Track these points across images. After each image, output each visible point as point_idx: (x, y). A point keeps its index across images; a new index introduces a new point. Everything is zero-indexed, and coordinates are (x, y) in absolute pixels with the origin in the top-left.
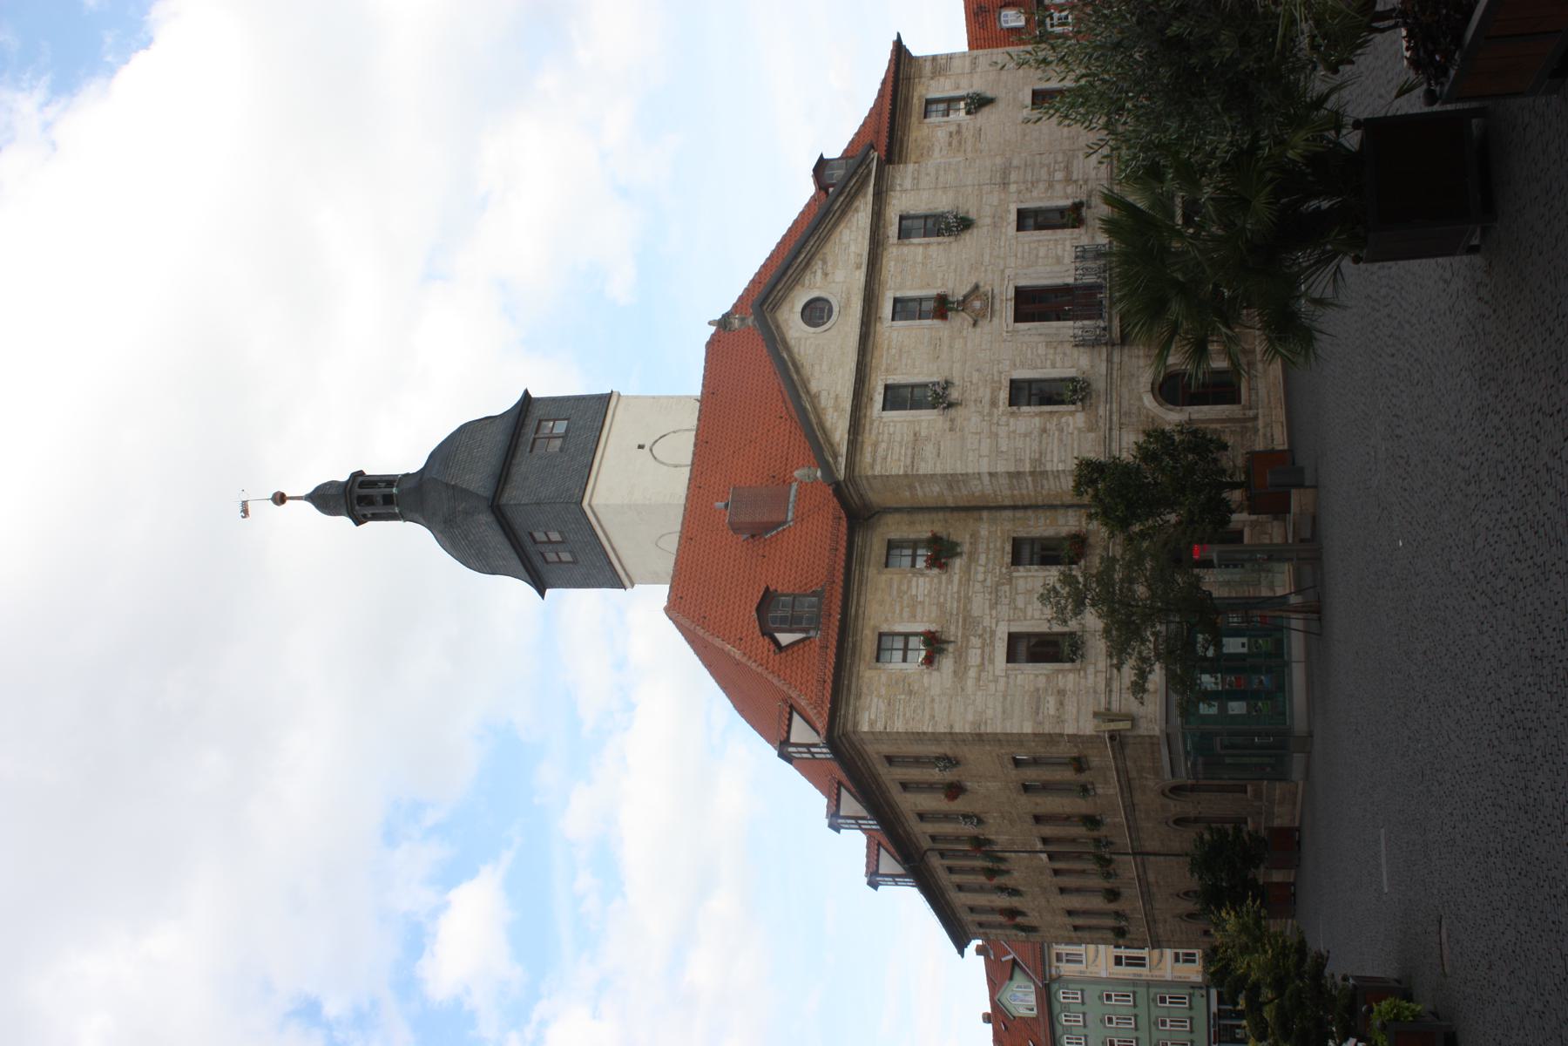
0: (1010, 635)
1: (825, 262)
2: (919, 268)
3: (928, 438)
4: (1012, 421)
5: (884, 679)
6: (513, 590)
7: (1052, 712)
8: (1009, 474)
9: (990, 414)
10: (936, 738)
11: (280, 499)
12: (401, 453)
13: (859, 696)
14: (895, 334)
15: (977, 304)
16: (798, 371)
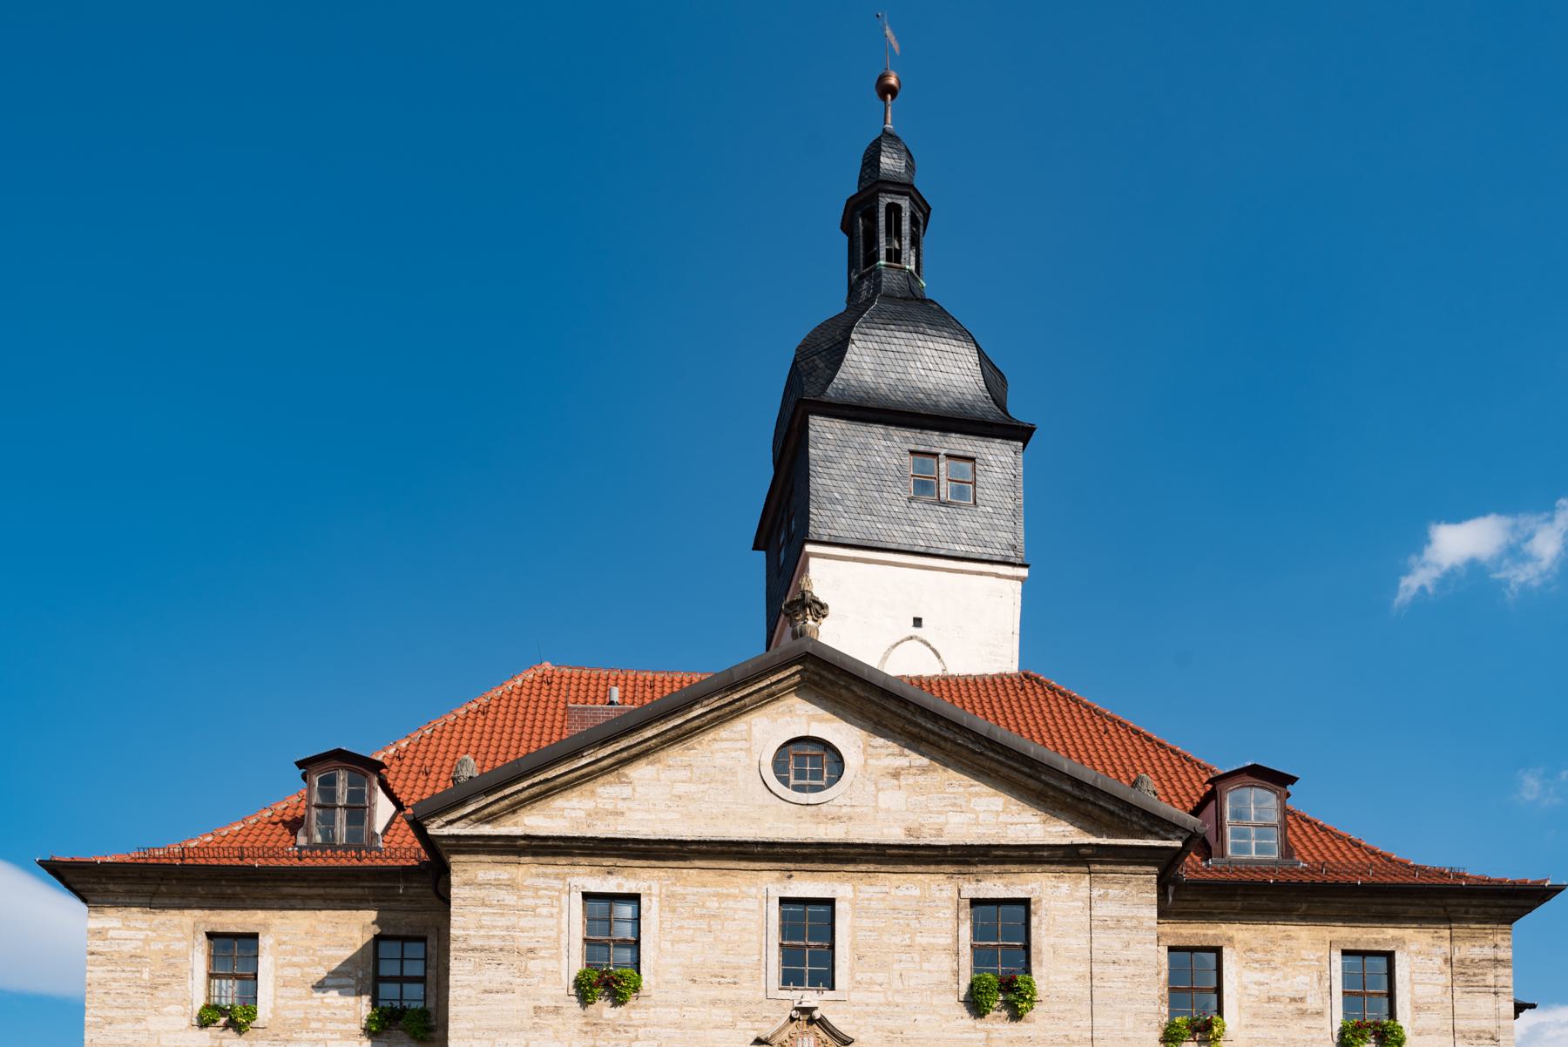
14: (752, 904)
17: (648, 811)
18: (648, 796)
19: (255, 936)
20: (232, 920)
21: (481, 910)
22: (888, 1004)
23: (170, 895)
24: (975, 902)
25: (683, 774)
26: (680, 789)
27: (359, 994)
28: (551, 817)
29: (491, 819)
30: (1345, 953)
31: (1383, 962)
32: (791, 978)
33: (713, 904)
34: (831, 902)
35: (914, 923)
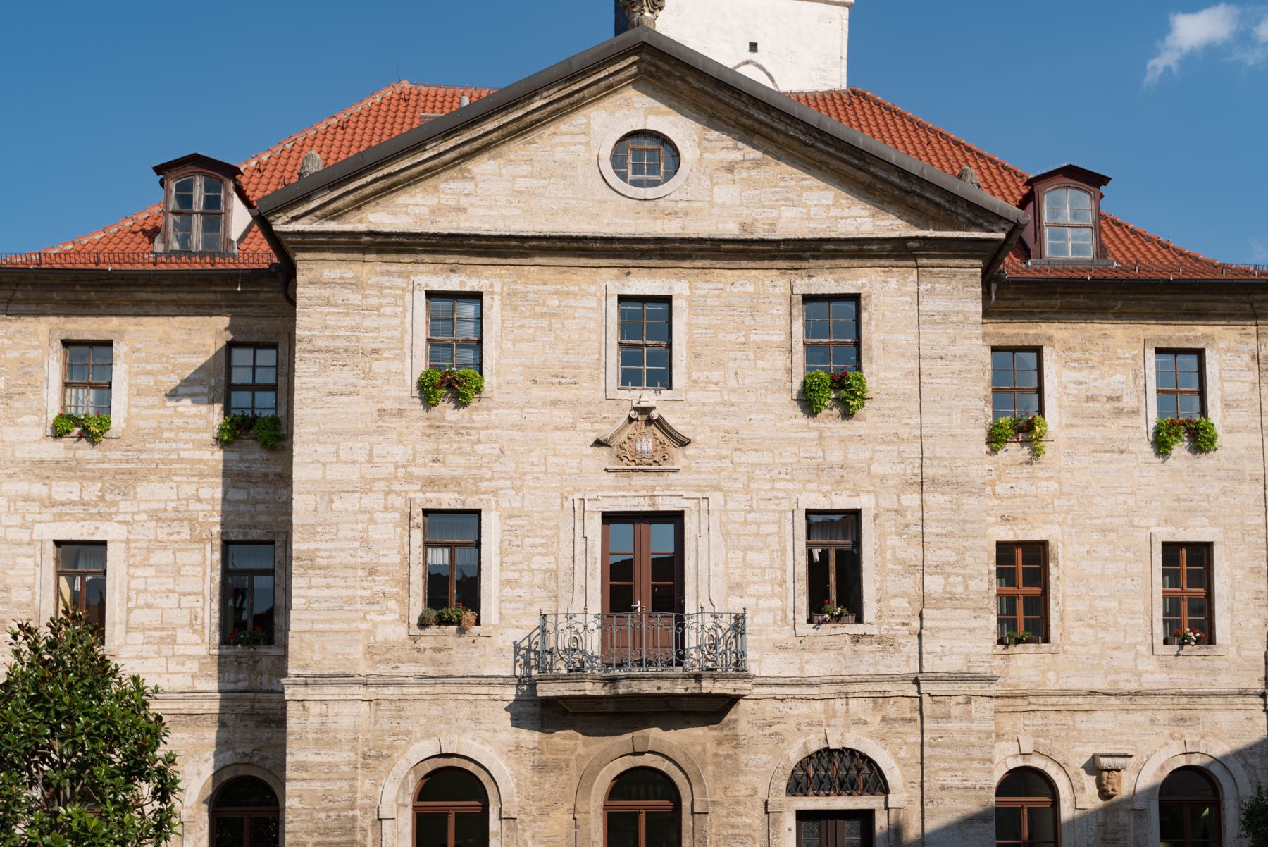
2: (739, 334)
3: (369, 374)
4: (396, 516)
5: (33, 354)
9: (409, 478)
14: (591, 302)
19: (109, 344)
20: (87, 327)
21: (326, 310)
22: (724, 404)
23: (27, 302)
24: (808, 299)
25: (525, 169)
26: (522, 184)
27: (212, 402)
28: (394, 213)
29: (336, 215)
30: (1159, 351)
31: (1192, 360)
32: (629, 378)
33: (554, 302)
34: (667, 300)
35: (748, 320)
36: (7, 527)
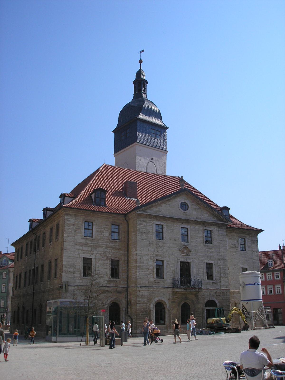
0: (91, 259)
1: (199, 209)
6: (114, 123)
7: (69, 270)
8: (136, 259)
9: (154, 254)
10: (63, 237)
11: (141, 61)
12: (153, 95)
13: (75, 216)
14: (178, 228)
15: (186, 251)
16: (167, 200)
17: (164, 211)
18: (164, 209)
21: (142, 225)
36: (75, 254)
